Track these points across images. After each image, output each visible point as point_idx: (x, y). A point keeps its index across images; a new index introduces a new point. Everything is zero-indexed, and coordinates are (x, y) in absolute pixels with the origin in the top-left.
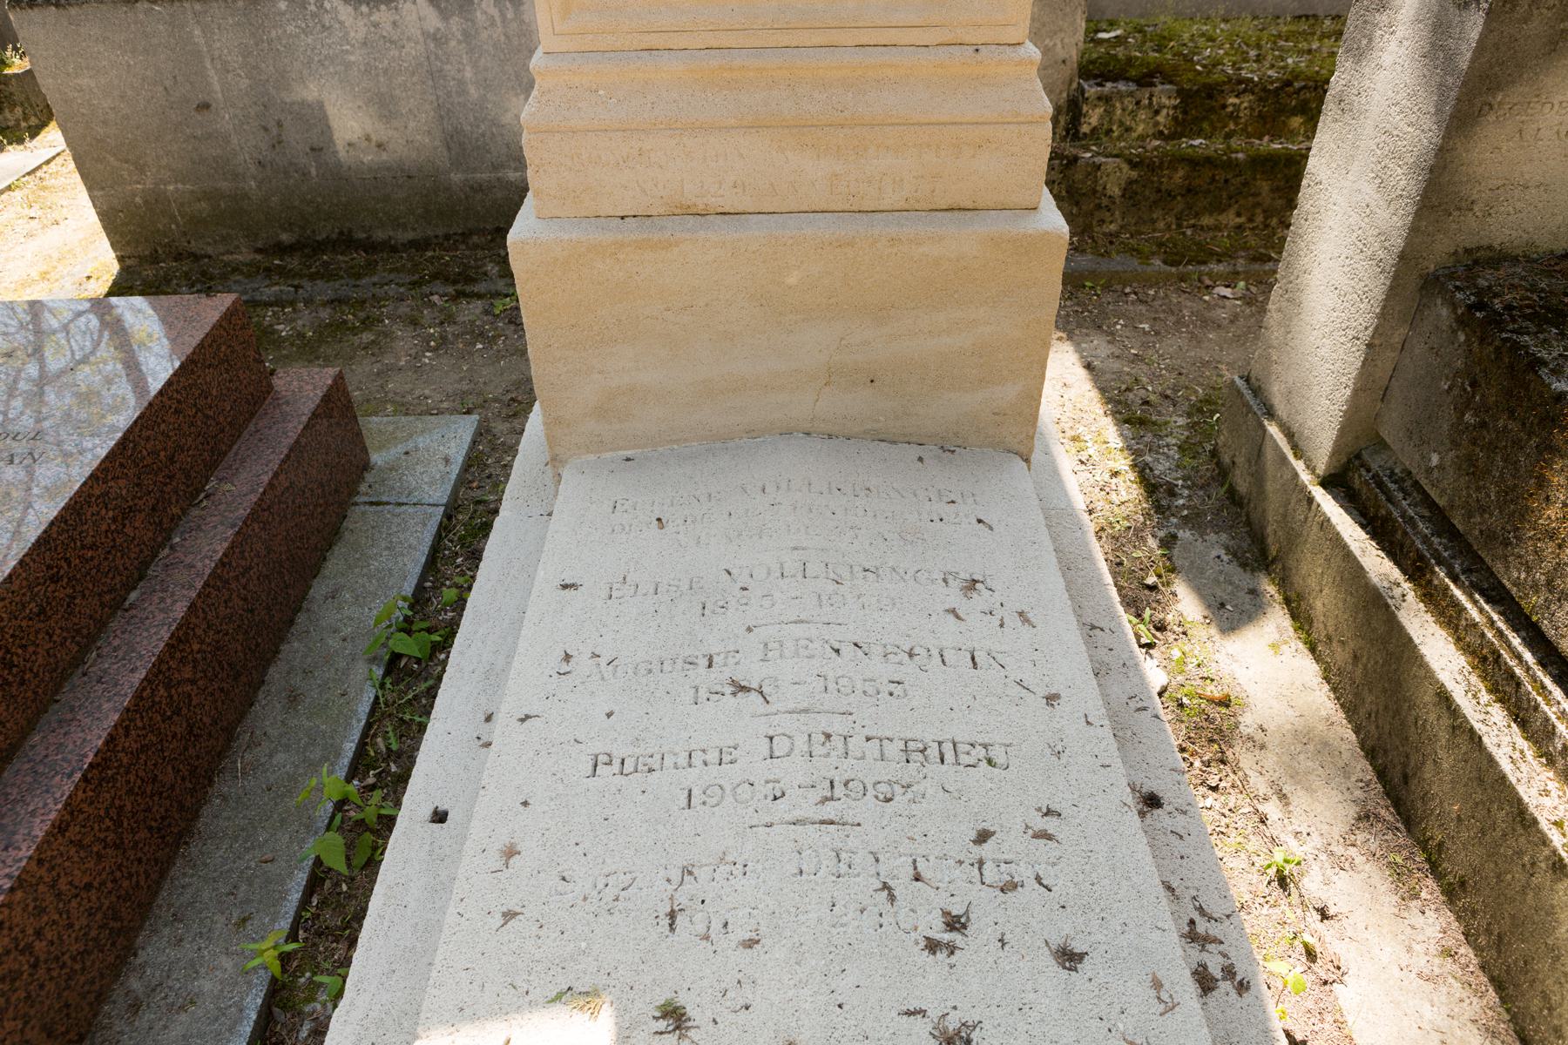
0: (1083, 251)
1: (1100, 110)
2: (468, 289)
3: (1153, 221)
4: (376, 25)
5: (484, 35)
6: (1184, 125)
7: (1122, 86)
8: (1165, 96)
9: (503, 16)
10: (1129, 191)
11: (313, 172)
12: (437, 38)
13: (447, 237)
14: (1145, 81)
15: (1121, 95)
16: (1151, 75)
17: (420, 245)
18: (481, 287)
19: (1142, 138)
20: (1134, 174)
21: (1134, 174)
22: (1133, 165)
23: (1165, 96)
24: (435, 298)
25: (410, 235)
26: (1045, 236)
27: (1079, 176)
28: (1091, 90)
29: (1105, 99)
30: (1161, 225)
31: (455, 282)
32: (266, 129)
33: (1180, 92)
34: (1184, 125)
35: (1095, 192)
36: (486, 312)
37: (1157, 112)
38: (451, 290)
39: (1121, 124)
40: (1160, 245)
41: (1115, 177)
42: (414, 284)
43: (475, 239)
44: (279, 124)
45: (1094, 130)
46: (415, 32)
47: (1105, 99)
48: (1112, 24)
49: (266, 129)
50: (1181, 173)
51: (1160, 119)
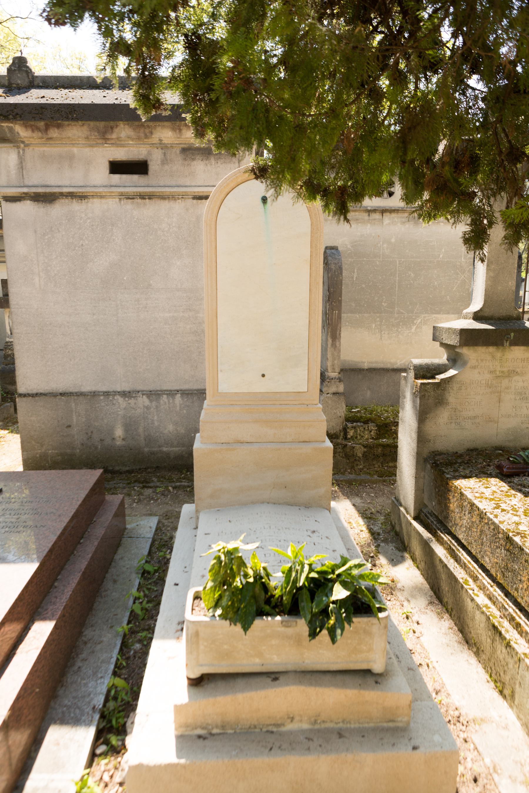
0: (352, 474)
1: (353, 431)
2: (147, 485)
3: (374, 465)
4: (129, 404)
5: (162, 407)
6: (379, 436)
7: (359, 424)
8: (372, 426)
9: (169, 401)
10: (364, 455)
11: (99, 447)
12: (148, 408)
13: (140, 469)
14: (366, 422)
15: (359, 427)
16: (368, 421)
17: (130, 472)
18: (151, 485)
19: (367, 439)
20: (365, 450)
21: (365, 450)
22: (365, 447)
23: (372, 426)
24: (136, 488)
25: (127, 468)
26: (327, 448)
27: (348, 450)
28: (349, 425)
29: (354, 428)
30: (376, 466)
31: (142, 483)
32: (87, 433)
33: (377, 426)
34: (379, 436)
35: (353, 455)
36: (154, 492)
37: (371, 432)
38: (141, 485)
39: (360, 435)
40: (377, 472)
41: (359, 451)
42: (129, 484)
43: (149, 470)
44: (92, 432)
45: (352, 437)
46: (141, 406)
47: (354, 428)
48: (357, 407)
49: (87, 433)
50: (380, 449)
51: (372, 433)
